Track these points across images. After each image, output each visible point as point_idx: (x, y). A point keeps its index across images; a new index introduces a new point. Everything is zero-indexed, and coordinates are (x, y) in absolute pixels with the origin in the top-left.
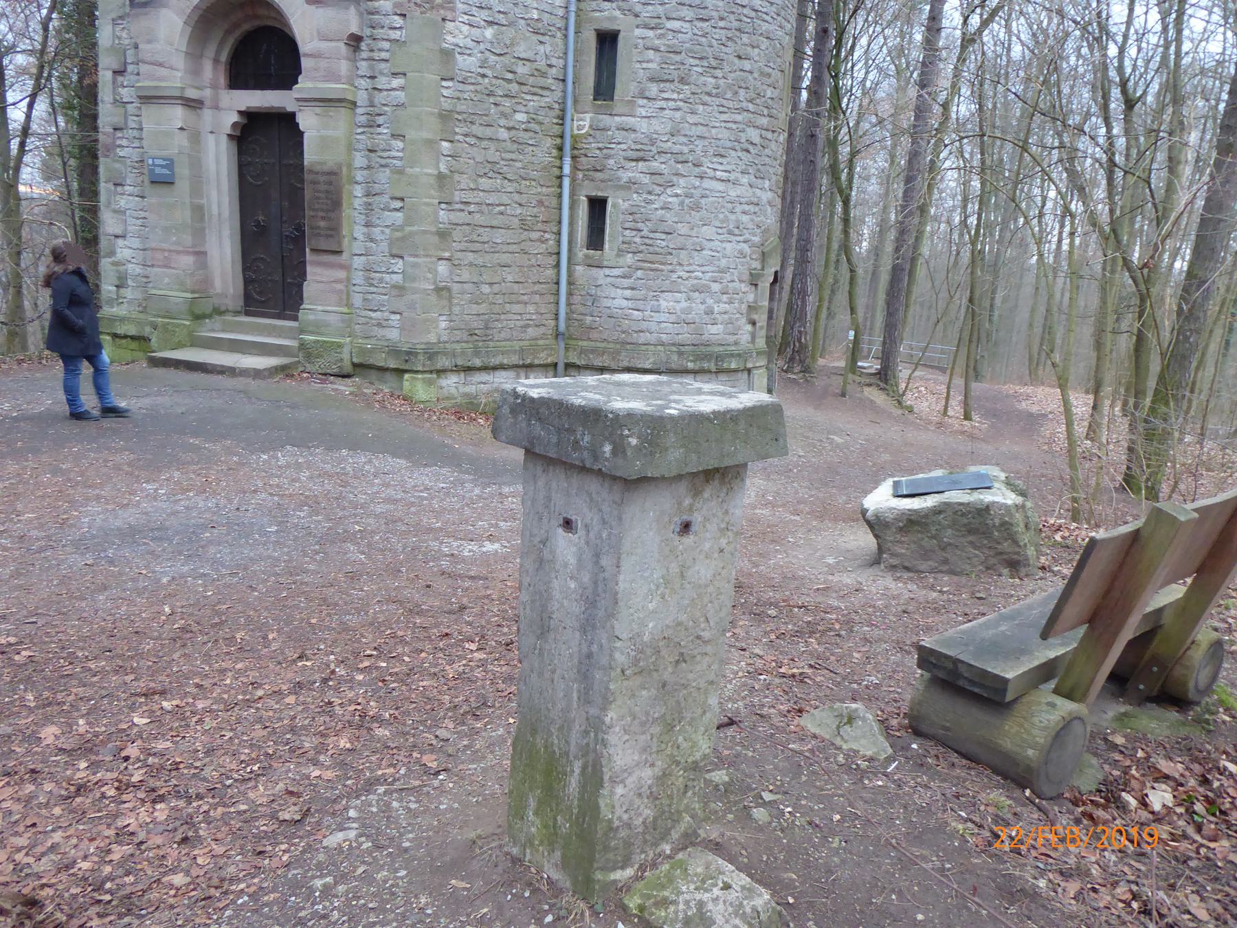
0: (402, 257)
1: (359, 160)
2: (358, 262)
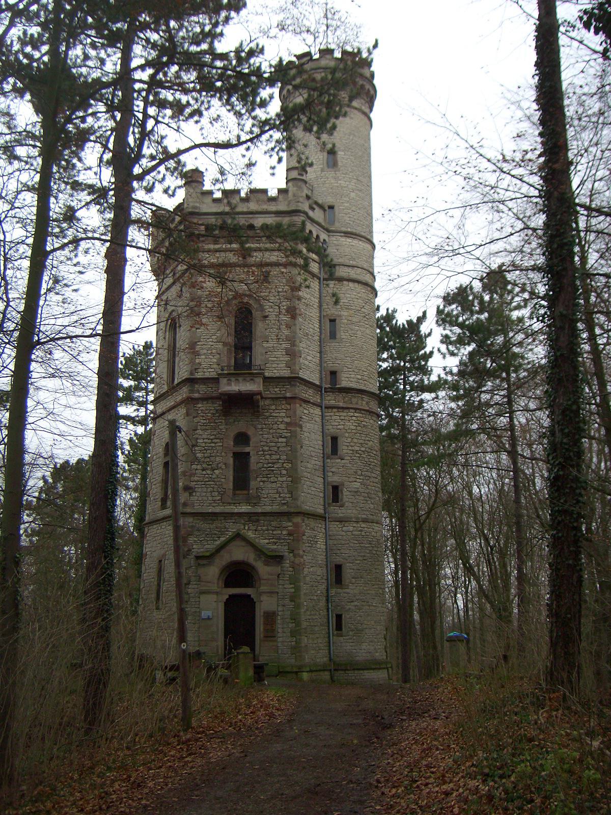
2: (280, 640)
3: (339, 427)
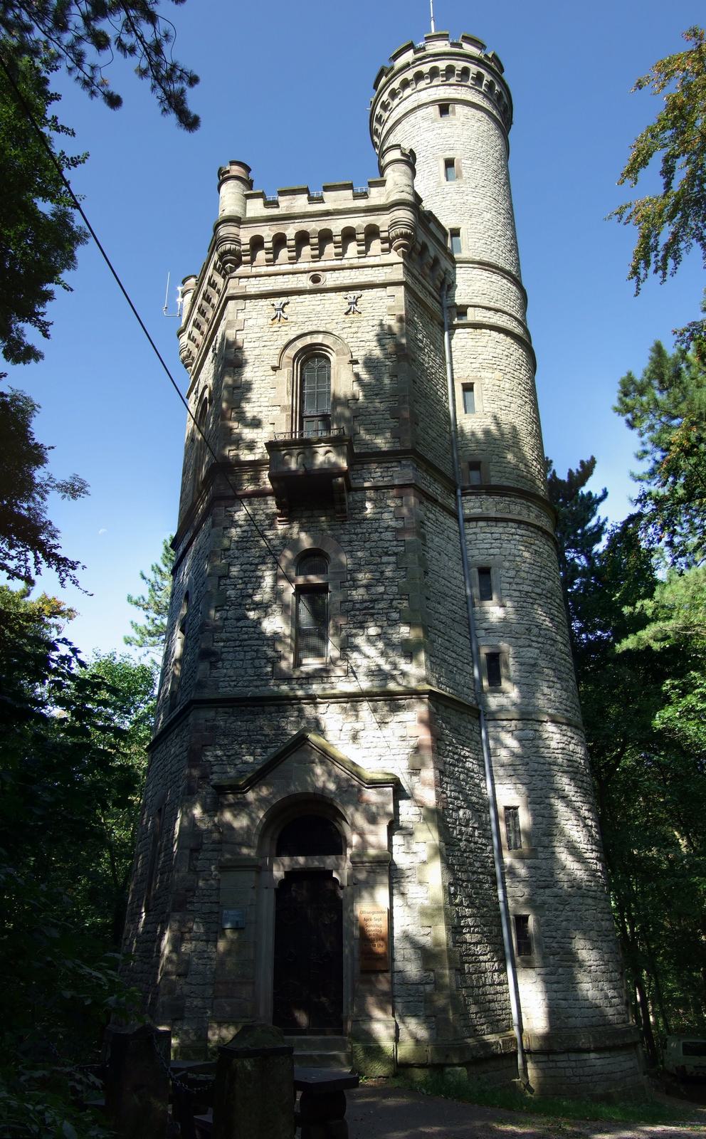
0: (433, 971)
3: (492, 551)
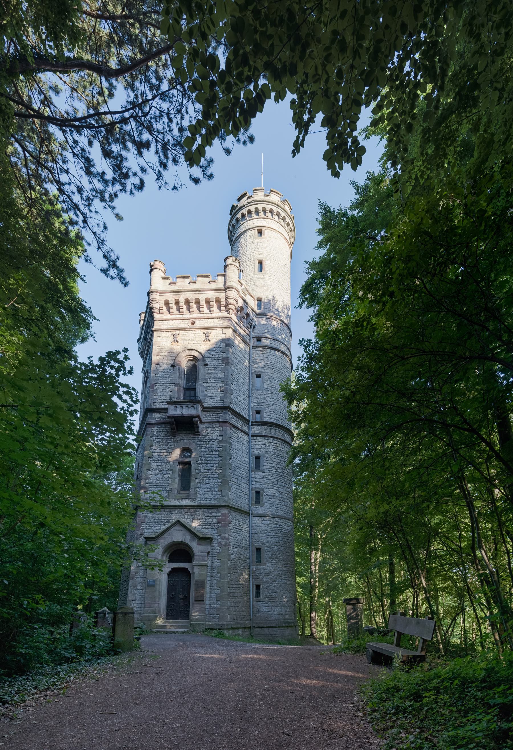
1: (208, 579)
